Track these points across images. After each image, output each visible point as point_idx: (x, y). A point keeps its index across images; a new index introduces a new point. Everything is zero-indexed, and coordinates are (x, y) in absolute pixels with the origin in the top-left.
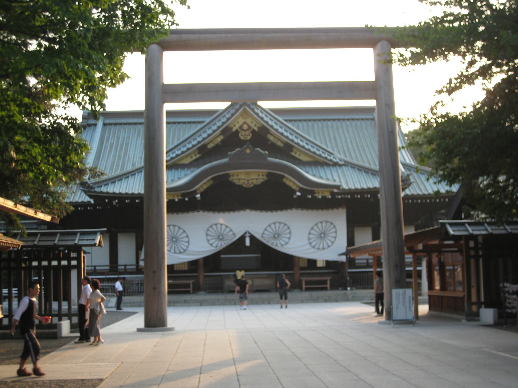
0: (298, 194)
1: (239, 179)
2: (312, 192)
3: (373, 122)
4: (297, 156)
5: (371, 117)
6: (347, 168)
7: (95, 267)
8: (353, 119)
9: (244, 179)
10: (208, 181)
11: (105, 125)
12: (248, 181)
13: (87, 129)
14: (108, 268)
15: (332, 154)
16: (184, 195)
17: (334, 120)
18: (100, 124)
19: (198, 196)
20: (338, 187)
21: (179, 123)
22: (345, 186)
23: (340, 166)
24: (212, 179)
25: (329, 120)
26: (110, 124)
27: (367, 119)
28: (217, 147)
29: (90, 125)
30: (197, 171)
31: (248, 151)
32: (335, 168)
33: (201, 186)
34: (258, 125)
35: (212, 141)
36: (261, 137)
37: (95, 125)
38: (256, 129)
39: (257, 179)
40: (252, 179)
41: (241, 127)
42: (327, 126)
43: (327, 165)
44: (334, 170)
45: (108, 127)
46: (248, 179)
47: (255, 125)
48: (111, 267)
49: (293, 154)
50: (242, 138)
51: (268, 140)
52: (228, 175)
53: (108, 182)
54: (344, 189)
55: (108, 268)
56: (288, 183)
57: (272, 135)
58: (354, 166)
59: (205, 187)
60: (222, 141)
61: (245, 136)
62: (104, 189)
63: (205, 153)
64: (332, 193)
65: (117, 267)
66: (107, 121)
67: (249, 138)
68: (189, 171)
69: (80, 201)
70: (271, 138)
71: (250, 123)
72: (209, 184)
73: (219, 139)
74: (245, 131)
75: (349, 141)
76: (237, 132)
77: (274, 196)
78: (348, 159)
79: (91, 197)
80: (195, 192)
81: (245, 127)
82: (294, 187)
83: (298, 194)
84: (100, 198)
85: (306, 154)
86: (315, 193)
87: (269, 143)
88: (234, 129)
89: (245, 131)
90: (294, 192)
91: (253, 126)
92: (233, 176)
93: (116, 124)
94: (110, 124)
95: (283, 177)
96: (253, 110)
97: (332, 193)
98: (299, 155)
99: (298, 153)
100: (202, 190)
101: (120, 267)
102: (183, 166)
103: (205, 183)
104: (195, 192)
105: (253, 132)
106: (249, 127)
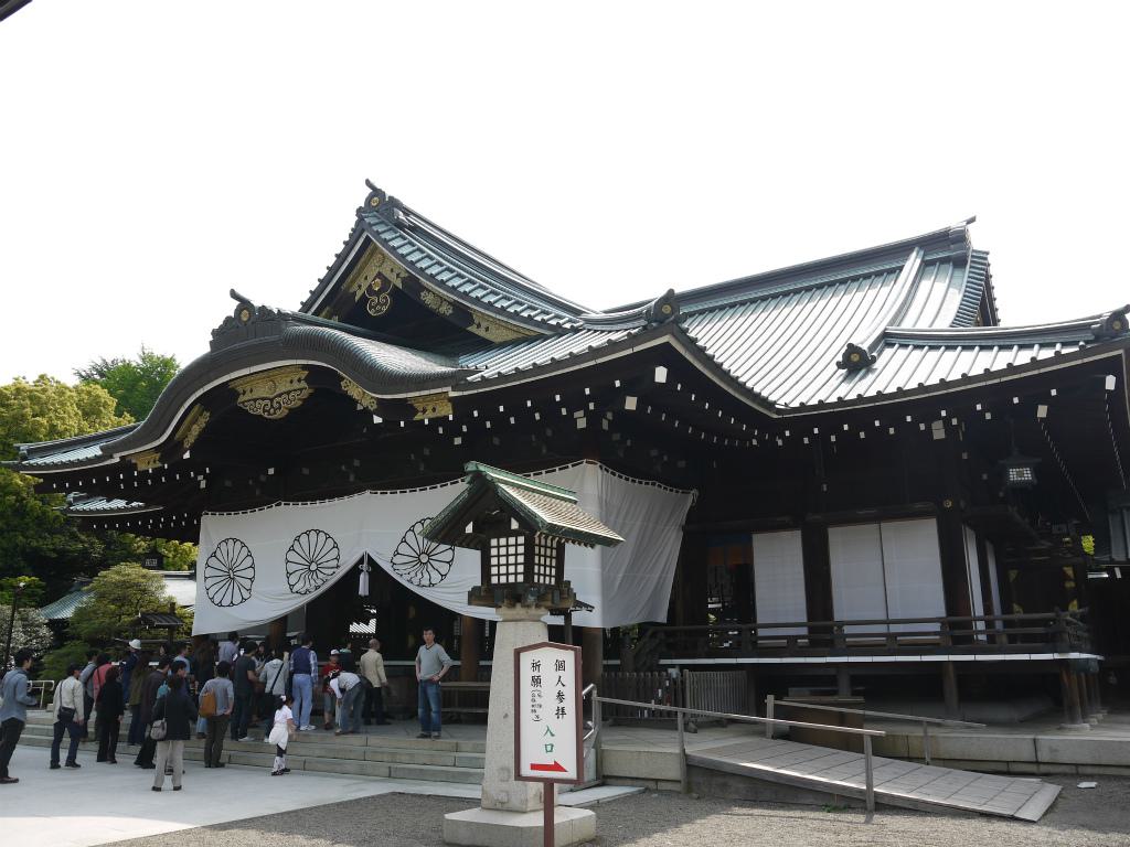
0: (377, 420)
1: (255, 400)
4: (481, 333)
9: (263, 399)
12: (272, 400)
34: (403, 275)
39: (288, 393)
40: (280, 395)
43: (543, 338)
46: (271, 396)
47: (398, 275)
49: (472, 329)
52: (227, 393)
59: (196, 430)
61: (378, 307)
67: (385, 309)
70: (428, 299)
72: (203, 422)
74: (378, 294)
83: (377, 420)
86: (416, 412)
88: (359, 295)
89: (378, 294)
91: (392, 278)
92: (244, 393)
98: (487, 329)
100: (191, 439)
106: (385, 281)
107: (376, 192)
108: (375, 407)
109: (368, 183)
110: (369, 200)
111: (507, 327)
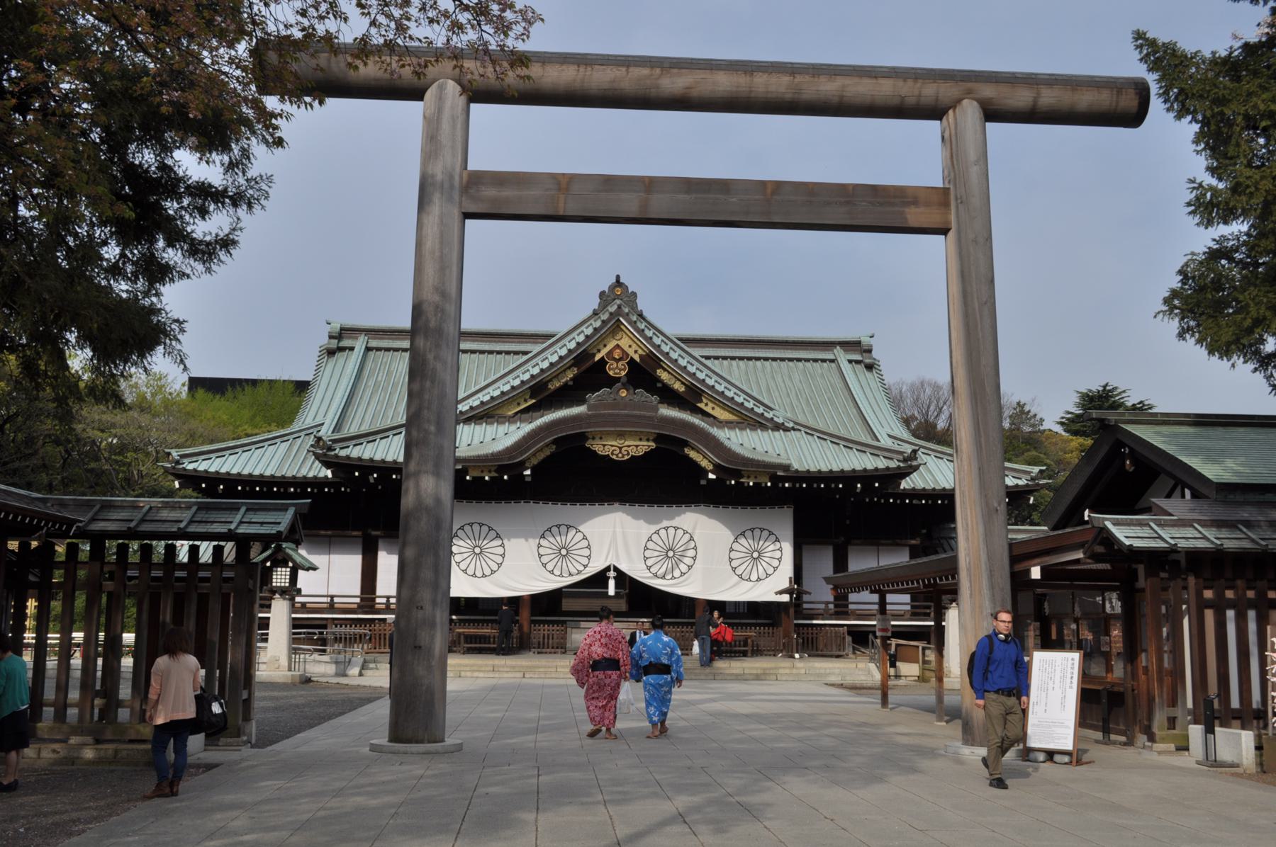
0: (711, 476)
2: (737, 474)
3: (833, 365)
4: (708, 409)
5: (832, 357)
6: (798, 433)
7: (332, 597)
8: (799, 360)
10: (547, 445)
11: (368, 349)
13: (338, 355)
14: (358, 600)
15: (771, 409)
16: (502, 469)
17: (766, 359)
18: (360, 344)
19: (528, 472)
20: (786, 468)
21: (499, 353)
22: (796, 466)
23: (787, 430)
24: (555, 442)
25: (758, 359)
26: (378, 349)
27: (824, 361)
28: (565, 387)
29: (341, 349)
30: (527, 428)
31: (623, 393)
32: (776, 434)
33: (534, 455)
34: (640, 352)
35: (557, 376)
36: (643, 374)
37: (352, 349)
38: (637, 358)
41: (610, 353)
42: (755, 366)
43: (763, 427)
44: (779, 435)
45: (372, 354)
48: (362, 600)
49: (701, 405)
50: (611, 373)
51: (658, 380)
52: (583, 437)
53: (361, 440)
54: (797, 471)
55: (358, 600)
56: (693, 454)
57: (665, 370)
58: (810, 431)
59: (541, 456)
60: (574, 379)
62: (355, 452)
63: (542, 394)
64: (774, 478)
65: (374, 599)
66: (374, 343)
68: (513, 427)
69: (311, 475)
70: (664, 376)
71: (626, 348)
72: (547, 452)
73: (570, 375)
75: (793, 395)
76: (603, 362)
77: (667, 478)
78: (801, 419)
79: (327, 465)
80: (522, 465)
81: (617, 355)
82: (704, 463)
83: (711, 476)
84: (343, 467)
85: (725, 407)
87: (659, 385)
88: (597, 358)
89: (617, 361)
90: (705, 472)
91: (631, 352)
93: (388, 350)
94: (378, 349)
95: (685, 444)
96: (633, 324)
97: (774, 478)
99: (711, 405)
100: (535, 461)
101: (378, 600)
102: (501, 419)
103: (541, 450)
104: (522, 465)
105: (632, 362)
107: (618, 283)
108: (711, 467)
109: (618, 277)
110: (612, 288)
111: (732, 411)
